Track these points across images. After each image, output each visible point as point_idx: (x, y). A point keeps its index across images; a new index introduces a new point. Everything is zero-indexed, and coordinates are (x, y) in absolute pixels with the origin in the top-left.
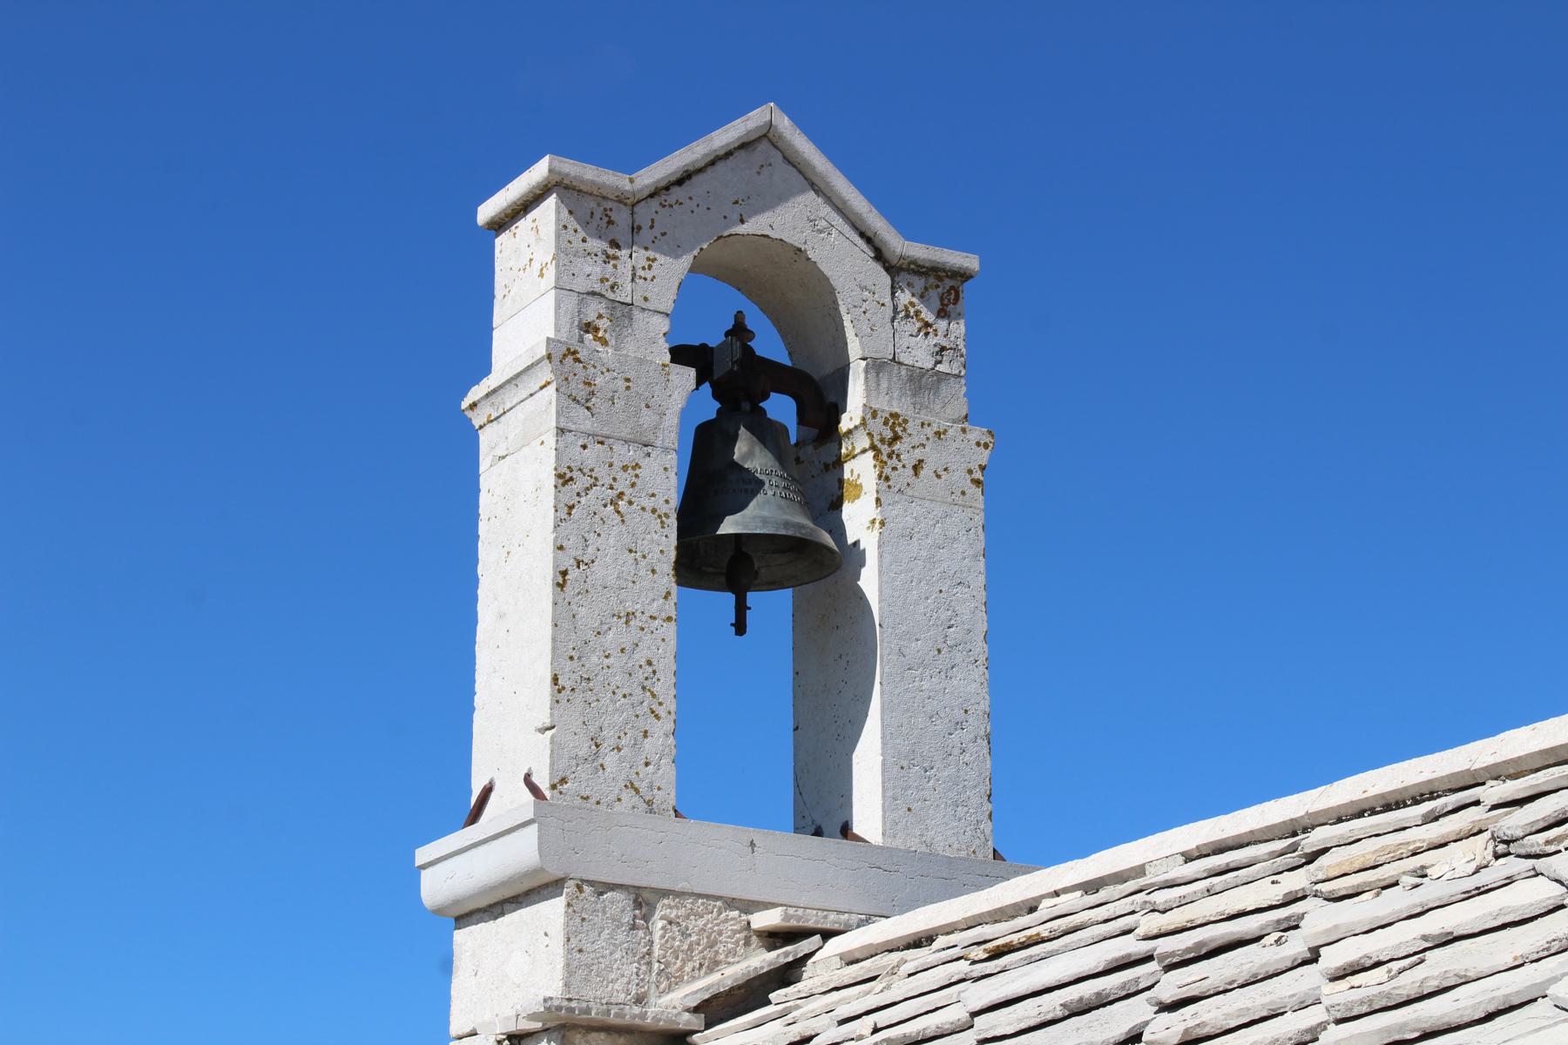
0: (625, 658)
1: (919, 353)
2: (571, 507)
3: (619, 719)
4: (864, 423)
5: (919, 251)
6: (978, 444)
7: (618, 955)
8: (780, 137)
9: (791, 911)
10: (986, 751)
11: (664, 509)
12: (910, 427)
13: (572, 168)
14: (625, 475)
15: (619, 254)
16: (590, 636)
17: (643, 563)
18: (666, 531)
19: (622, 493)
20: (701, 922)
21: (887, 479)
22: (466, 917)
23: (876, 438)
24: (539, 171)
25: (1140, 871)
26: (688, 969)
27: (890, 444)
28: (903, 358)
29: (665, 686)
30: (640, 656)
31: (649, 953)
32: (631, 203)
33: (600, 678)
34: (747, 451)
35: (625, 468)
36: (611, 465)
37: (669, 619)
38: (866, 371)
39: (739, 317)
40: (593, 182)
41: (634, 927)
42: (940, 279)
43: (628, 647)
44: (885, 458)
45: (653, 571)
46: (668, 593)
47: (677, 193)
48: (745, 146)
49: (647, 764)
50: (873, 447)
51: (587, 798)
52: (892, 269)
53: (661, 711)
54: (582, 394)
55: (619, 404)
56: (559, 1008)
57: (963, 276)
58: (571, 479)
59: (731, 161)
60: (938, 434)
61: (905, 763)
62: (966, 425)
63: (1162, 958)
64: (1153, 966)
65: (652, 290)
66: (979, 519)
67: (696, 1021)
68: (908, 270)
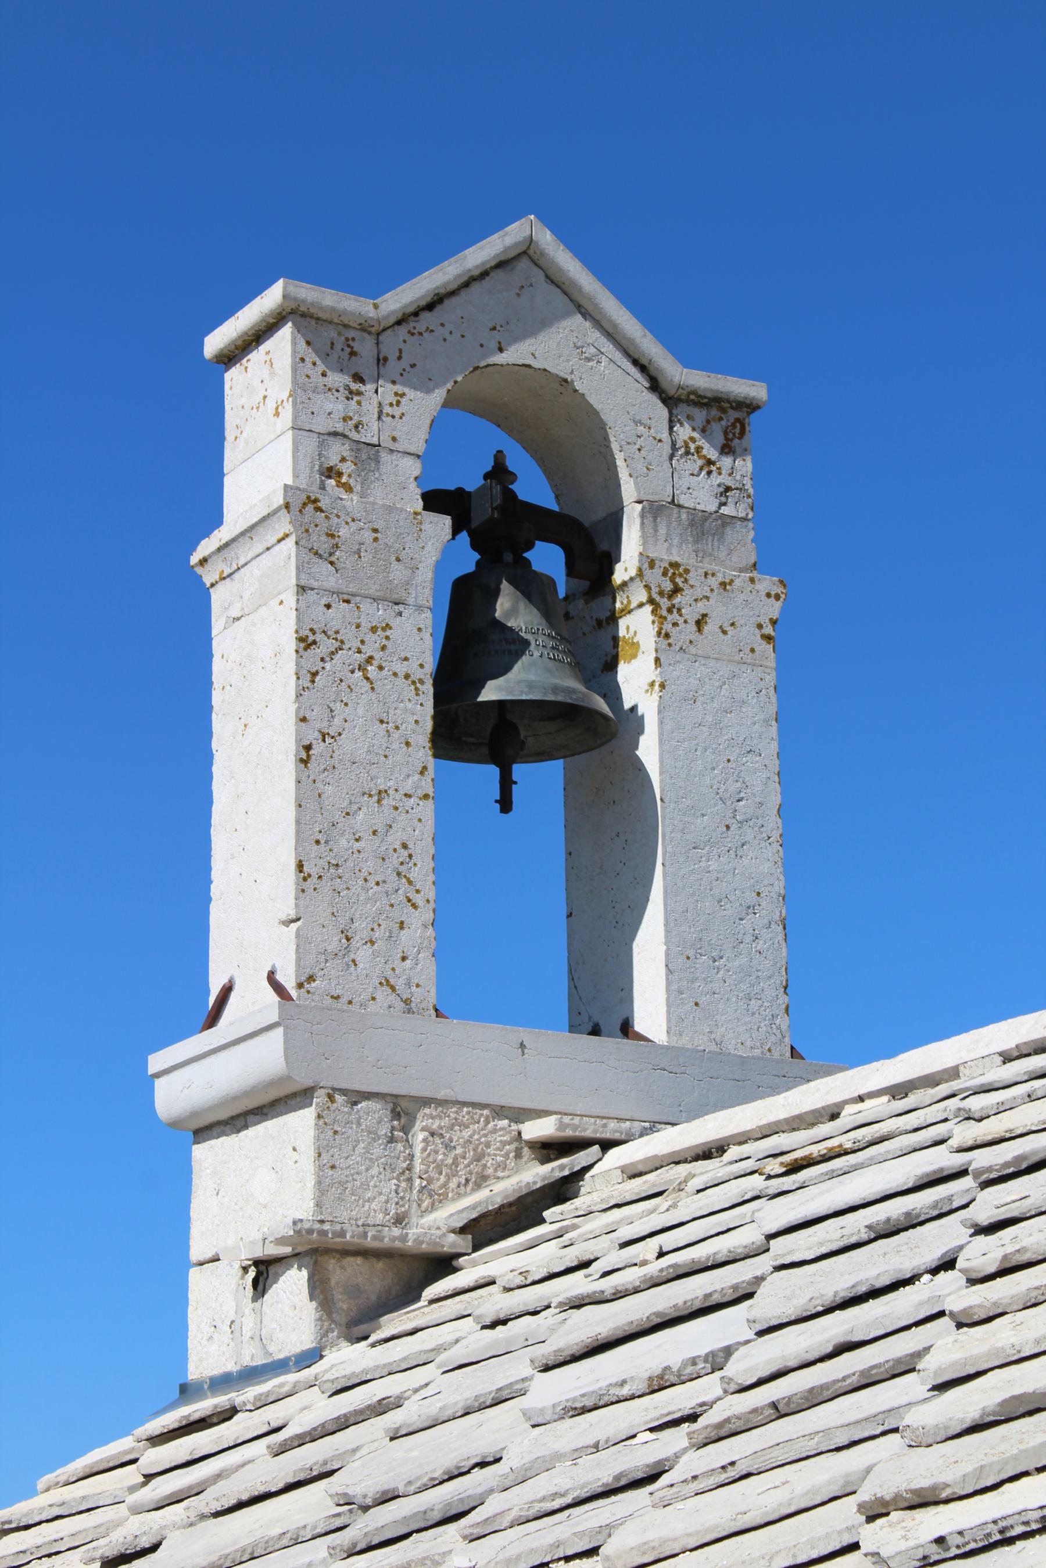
0: (377, 840)
1: (701, 494)
2: (315, 674)
3: (372, 909)
4: (640, 573)
6: (768, 595)
7: (374, 1171)
8: (542, 254)
9: (566, 1119)
10: (781, 937)
11: (418, 674)
12: (693, 578)
13: (308, 293)
14: (374, 637)
15: (363, 388)
16: (338, 817)
17: (396, 735)
18: (421, 698)
19: (371, 658)
20: (466, 1133)
21: (667, 636)
22: (203, 1132)
23: (655, 590)
24: (272, 298)
25: (953, 1073)
26: (452, 1185)
27: (670, 597)
28: (684, 500)
29: (422, 872)
30: (395, 838)
31: (409, 1168)
32: (377, 332)
33: (350, 864)
34: (510, 608)
35: (374, 629)
36: (358, 626)
37: (426, 797)
38: (643, 515)
39: (499, 457)
40: (333, 309)
41: (392, 1140)
42: (723, 410)
43: (381, 829)
44: (664, 613)
45: (408, 744)
46: (425, 768)
47: (427, 319)
48: (502, 264)
49: (404, 959)
50: (651, 601)
51: (338, 998)
52: (669, 400)
53: (419, 900)
54: (324, 546)
55: (366, 557)
56: (310, 1231)
57: (749, 407)
58: (314, 642)
59: (487, 282)
60: (723, 585)
61: (691, 953)
62: (755, 574)
63: (977, 1175)
64: (967, 1183)
65: (400, 429)
66: (771, 679)
67: (463, 1243)
68: (688, 402)
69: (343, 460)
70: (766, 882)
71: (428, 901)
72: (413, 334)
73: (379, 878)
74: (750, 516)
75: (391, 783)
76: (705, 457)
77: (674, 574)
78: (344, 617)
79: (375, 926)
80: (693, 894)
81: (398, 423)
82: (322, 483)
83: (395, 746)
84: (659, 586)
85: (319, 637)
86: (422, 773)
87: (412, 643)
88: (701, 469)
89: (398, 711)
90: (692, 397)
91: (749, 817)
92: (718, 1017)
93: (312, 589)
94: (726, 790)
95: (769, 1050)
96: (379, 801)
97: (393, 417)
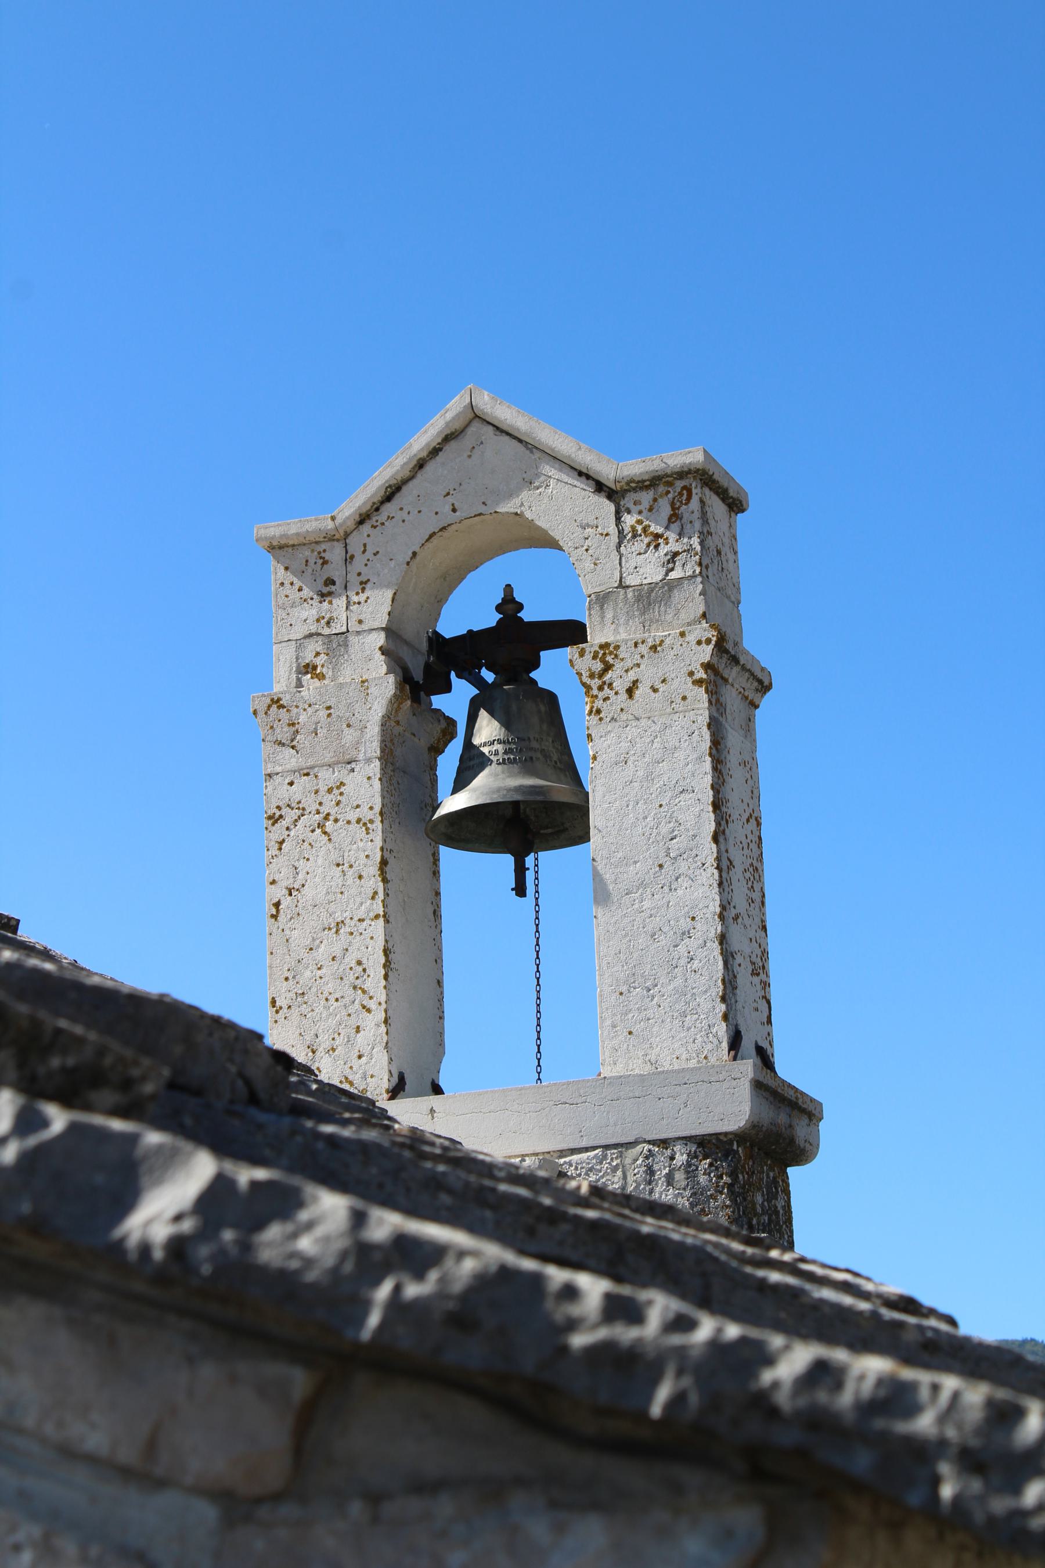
0: (336, 964)
3: (332, 1022)
5: (635, 468)
16: (303, 953)
17: (350, 873)
19: (328, 814)
27: (601, 676)
28: (630, 580)
30: (351, 960)
33: (314, 990)
35: (330, 791)
36: (316, 792)
40: (298, 534)
43: (338, 953)
44: (595, 692)
45: (360, 877)
46: (376, 893)
47: (389, 509)
49: (360, 1057)
52: (612, 494)
53: (372, 1004)
54: (285, 737)
58: (281, 816)
60: (654, 648)
61: (624, 989)
70: (701, 906)
71: (380, 1004)
72: (375, 527)
73: (338, 995)
74: (697, 572)
75: (347, 913)
76: (652, 533)
77: (604, 654)
78: (304, 788)
79: (336, 1035)
80: (626, 935)
81: (364, 607)
82: (299, 680)
83: (350, 882)
84: (590, 670)
86: (373, 898)
87: (362, 791)
88: (648, 545)
89: (352, 852)
90: (633, 485)
91: (682, 850)
92: (653, 1039)
93: (277, 774)
94: (658, 834)
95: (706, 1058)
96: (337, 932)
97: (359, 603)
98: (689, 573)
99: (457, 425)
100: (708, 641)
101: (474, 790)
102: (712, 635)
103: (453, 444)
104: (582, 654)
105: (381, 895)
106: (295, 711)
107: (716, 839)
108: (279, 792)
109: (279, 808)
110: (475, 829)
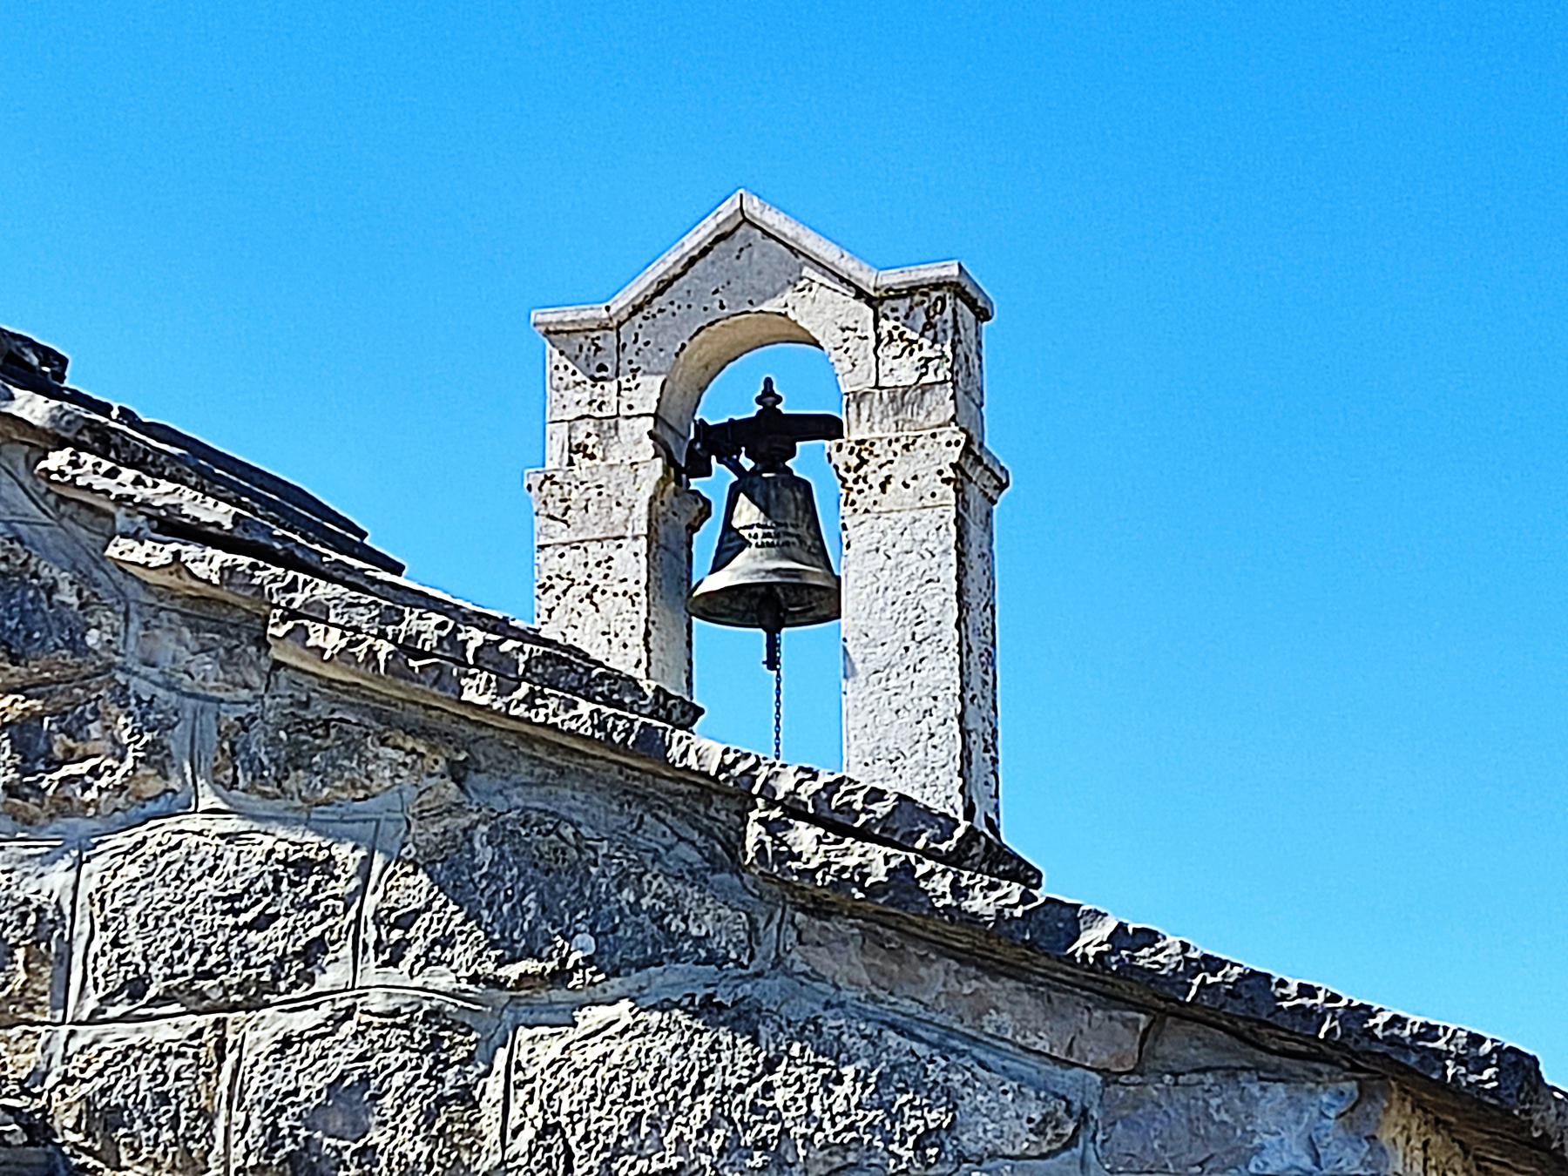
2: (550, 611)
5: (893, 278)
11: (633, 589)
35: (598, 564)
36: (586, 564)
46: (639, 662)
52: (870, 301)
60: (906, 447)
69: (589, 435)
82: (571, 459)
83: (615, 650)
85: (555, 581)
86: (637, 666)
88: (904, 350)
98: (941, 378)
99: (728, 228)
100: (957, 443)
101: (734, 570)
102: (962, 437)
103: (722, 244)
104: (839, 448)
105: (644, 664)
106: (566, 488)
107: (958, 626)
108: (549, 564)
109: (550, 578)
110: (737, 606)
